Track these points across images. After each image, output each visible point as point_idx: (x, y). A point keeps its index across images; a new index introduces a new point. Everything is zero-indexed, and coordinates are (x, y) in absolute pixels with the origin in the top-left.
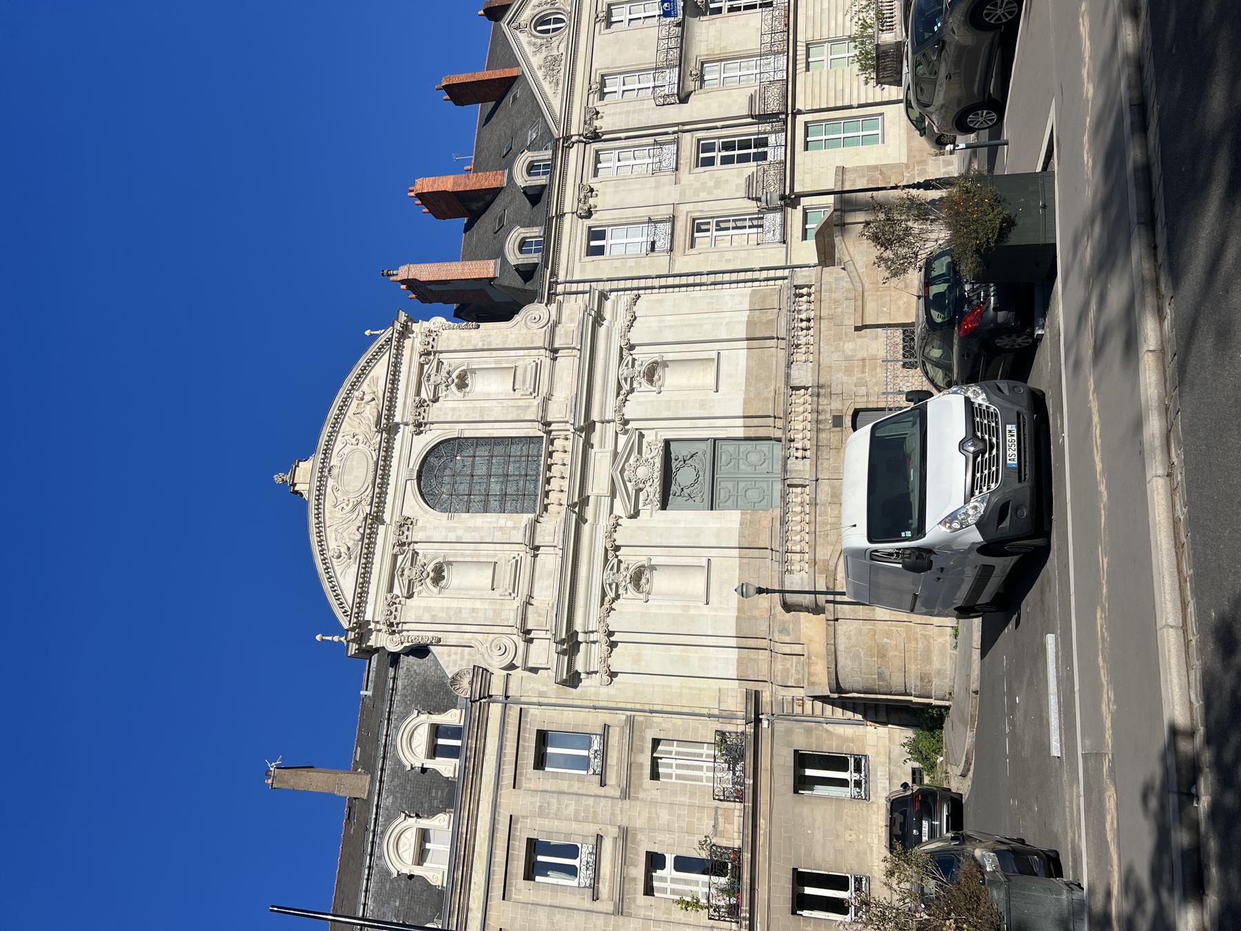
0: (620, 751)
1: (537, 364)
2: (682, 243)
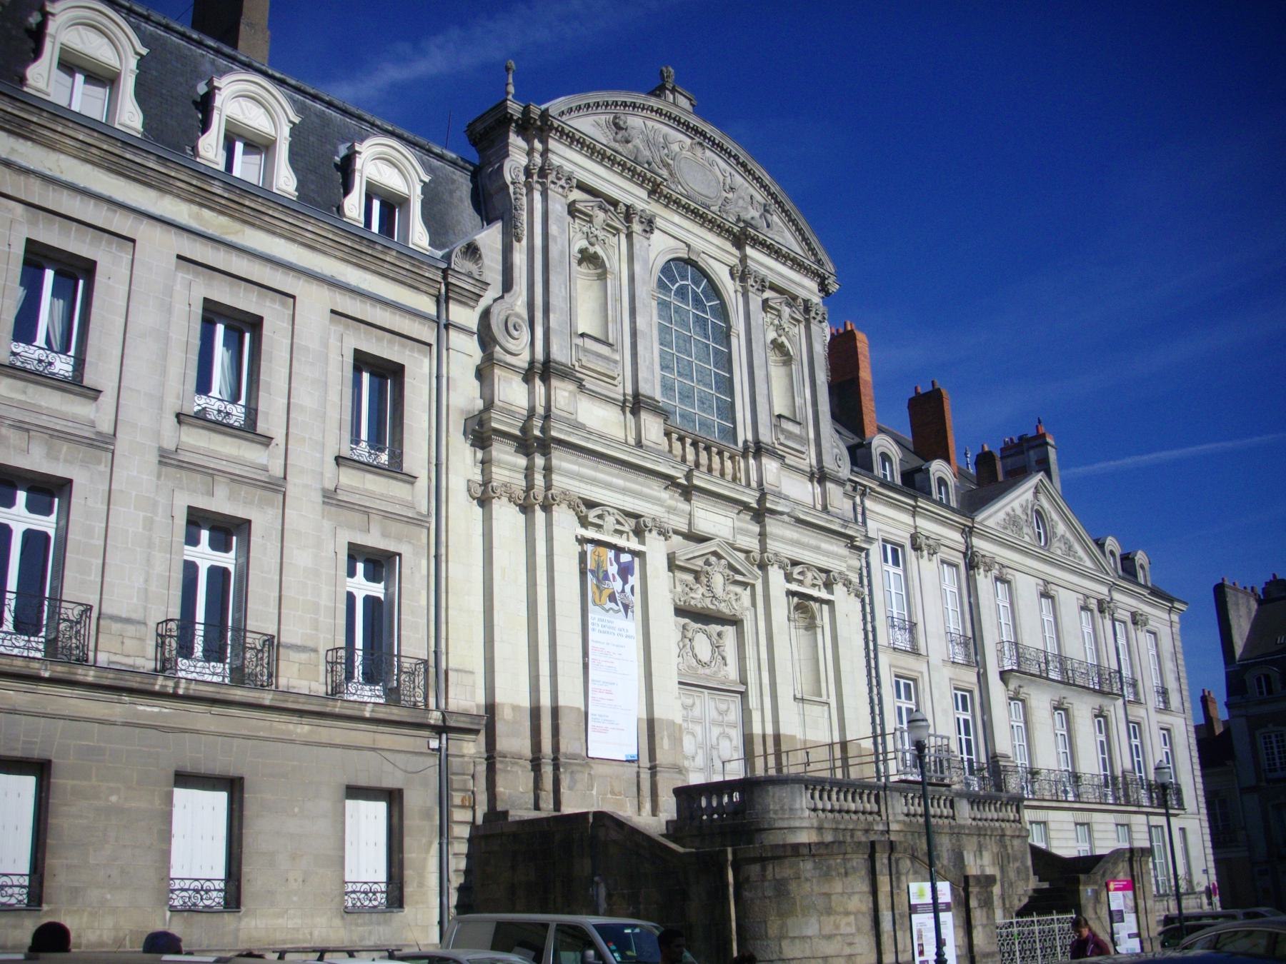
0: (382, 498)
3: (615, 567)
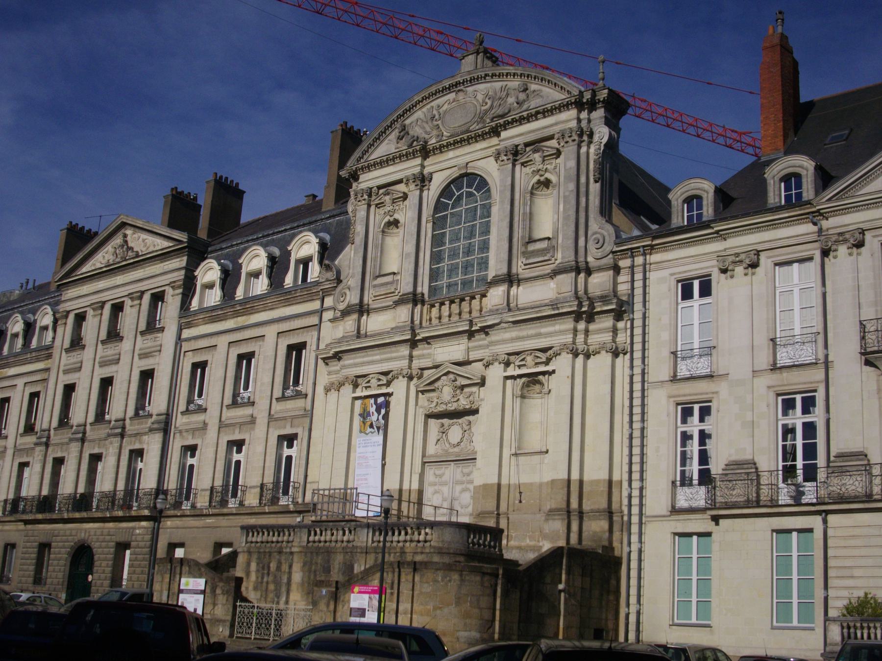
1: (549, 260)
2: (682, 392)
3: (374, 407)
